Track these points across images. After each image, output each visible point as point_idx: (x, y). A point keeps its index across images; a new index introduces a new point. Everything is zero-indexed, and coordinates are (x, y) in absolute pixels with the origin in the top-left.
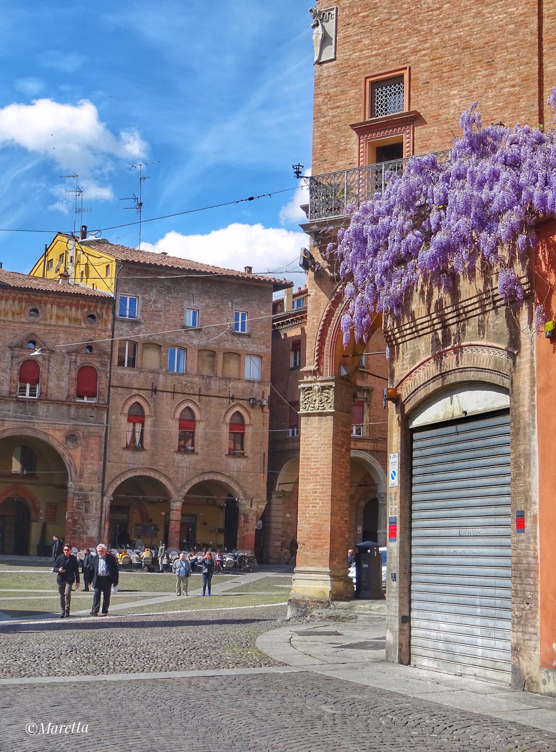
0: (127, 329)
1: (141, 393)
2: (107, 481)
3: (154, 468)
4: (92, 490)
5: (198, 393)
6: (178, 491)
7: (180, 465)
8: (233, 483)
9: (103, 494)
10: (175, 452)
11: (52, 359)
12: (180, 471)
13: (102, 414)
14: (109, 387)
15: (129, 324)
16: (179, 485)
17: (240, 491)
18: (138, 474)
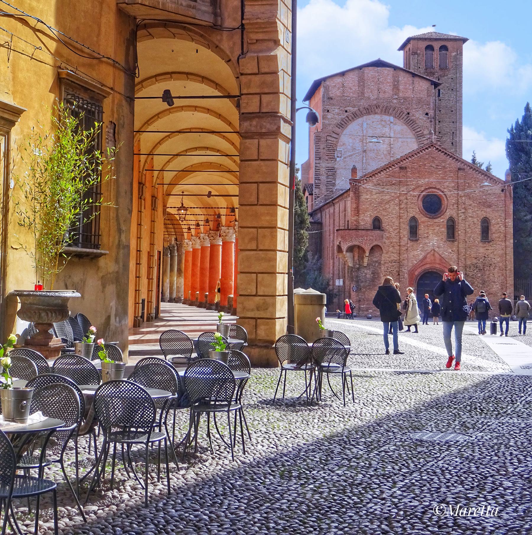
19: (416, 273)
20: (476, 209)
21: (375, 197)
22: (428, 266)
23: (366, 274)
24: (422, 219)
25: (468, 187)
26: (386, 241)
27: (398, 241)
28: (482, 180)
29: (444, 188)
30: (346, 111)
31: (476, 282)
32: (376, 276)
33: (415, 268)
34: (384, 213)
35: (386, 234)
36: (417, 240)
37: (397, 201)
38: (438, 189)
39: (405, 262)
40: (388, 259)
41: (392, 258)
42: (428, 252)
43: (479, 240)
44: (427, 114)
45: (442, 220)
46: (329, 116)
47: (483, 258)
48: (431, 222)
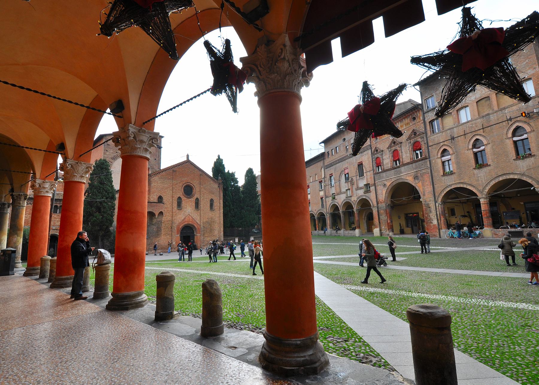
0: (431, 114)
1: (445, 143)
2: (437, 195)
3: (462, 181)
4: (430, 201)
5: (482, 128)
6: (482, 192)
7: (479, 176)
8: (525, 177)
9: (436, 202)
10: (474, 169)
11: (402, 146)
12: (480, 180)
13: (426, 162)
14: (428, 147)
15: (432, 111)
16: (481, 188)
17: (534, 182)
18: (453, 187)
21: (159, 185)
22: (186, 223)
23: (153, 228)
24: (183, 198)
26: (165, 209)
27: (171, 210)
30: (117, 152)
33: (180, 223)
36: (181, 209)
37: (171, 188)
38: (191, 184)
39: (175, 221)
41: (168, 219)
44: (155, 159)
45: (193, 199)
46: (107, 153)
48: (188, 200)
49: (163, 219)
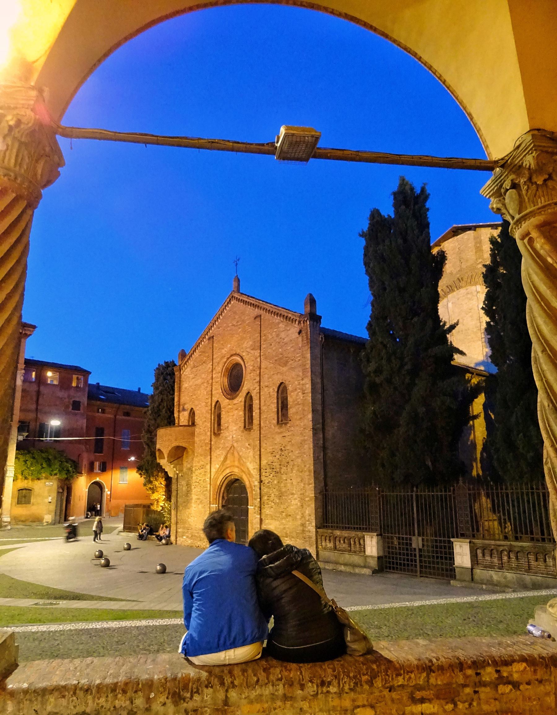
19: (218, 484)
20: (272, 373)
22: (228, 471)
24: (224, 402)
25: (265, 341)
28: (279, 323)
29: (243, 352)
31: (273, 495)
32: (189, 489)
34: (196, 402)
35: (197, 430)
40: (198, 465)
42: (228, 449)
43: (275, 422)
45: (240, 399)
47: (280, 452)
49: (194, 465)
